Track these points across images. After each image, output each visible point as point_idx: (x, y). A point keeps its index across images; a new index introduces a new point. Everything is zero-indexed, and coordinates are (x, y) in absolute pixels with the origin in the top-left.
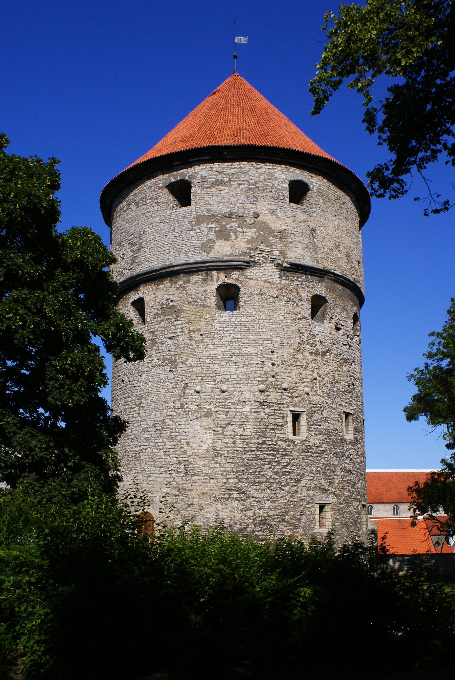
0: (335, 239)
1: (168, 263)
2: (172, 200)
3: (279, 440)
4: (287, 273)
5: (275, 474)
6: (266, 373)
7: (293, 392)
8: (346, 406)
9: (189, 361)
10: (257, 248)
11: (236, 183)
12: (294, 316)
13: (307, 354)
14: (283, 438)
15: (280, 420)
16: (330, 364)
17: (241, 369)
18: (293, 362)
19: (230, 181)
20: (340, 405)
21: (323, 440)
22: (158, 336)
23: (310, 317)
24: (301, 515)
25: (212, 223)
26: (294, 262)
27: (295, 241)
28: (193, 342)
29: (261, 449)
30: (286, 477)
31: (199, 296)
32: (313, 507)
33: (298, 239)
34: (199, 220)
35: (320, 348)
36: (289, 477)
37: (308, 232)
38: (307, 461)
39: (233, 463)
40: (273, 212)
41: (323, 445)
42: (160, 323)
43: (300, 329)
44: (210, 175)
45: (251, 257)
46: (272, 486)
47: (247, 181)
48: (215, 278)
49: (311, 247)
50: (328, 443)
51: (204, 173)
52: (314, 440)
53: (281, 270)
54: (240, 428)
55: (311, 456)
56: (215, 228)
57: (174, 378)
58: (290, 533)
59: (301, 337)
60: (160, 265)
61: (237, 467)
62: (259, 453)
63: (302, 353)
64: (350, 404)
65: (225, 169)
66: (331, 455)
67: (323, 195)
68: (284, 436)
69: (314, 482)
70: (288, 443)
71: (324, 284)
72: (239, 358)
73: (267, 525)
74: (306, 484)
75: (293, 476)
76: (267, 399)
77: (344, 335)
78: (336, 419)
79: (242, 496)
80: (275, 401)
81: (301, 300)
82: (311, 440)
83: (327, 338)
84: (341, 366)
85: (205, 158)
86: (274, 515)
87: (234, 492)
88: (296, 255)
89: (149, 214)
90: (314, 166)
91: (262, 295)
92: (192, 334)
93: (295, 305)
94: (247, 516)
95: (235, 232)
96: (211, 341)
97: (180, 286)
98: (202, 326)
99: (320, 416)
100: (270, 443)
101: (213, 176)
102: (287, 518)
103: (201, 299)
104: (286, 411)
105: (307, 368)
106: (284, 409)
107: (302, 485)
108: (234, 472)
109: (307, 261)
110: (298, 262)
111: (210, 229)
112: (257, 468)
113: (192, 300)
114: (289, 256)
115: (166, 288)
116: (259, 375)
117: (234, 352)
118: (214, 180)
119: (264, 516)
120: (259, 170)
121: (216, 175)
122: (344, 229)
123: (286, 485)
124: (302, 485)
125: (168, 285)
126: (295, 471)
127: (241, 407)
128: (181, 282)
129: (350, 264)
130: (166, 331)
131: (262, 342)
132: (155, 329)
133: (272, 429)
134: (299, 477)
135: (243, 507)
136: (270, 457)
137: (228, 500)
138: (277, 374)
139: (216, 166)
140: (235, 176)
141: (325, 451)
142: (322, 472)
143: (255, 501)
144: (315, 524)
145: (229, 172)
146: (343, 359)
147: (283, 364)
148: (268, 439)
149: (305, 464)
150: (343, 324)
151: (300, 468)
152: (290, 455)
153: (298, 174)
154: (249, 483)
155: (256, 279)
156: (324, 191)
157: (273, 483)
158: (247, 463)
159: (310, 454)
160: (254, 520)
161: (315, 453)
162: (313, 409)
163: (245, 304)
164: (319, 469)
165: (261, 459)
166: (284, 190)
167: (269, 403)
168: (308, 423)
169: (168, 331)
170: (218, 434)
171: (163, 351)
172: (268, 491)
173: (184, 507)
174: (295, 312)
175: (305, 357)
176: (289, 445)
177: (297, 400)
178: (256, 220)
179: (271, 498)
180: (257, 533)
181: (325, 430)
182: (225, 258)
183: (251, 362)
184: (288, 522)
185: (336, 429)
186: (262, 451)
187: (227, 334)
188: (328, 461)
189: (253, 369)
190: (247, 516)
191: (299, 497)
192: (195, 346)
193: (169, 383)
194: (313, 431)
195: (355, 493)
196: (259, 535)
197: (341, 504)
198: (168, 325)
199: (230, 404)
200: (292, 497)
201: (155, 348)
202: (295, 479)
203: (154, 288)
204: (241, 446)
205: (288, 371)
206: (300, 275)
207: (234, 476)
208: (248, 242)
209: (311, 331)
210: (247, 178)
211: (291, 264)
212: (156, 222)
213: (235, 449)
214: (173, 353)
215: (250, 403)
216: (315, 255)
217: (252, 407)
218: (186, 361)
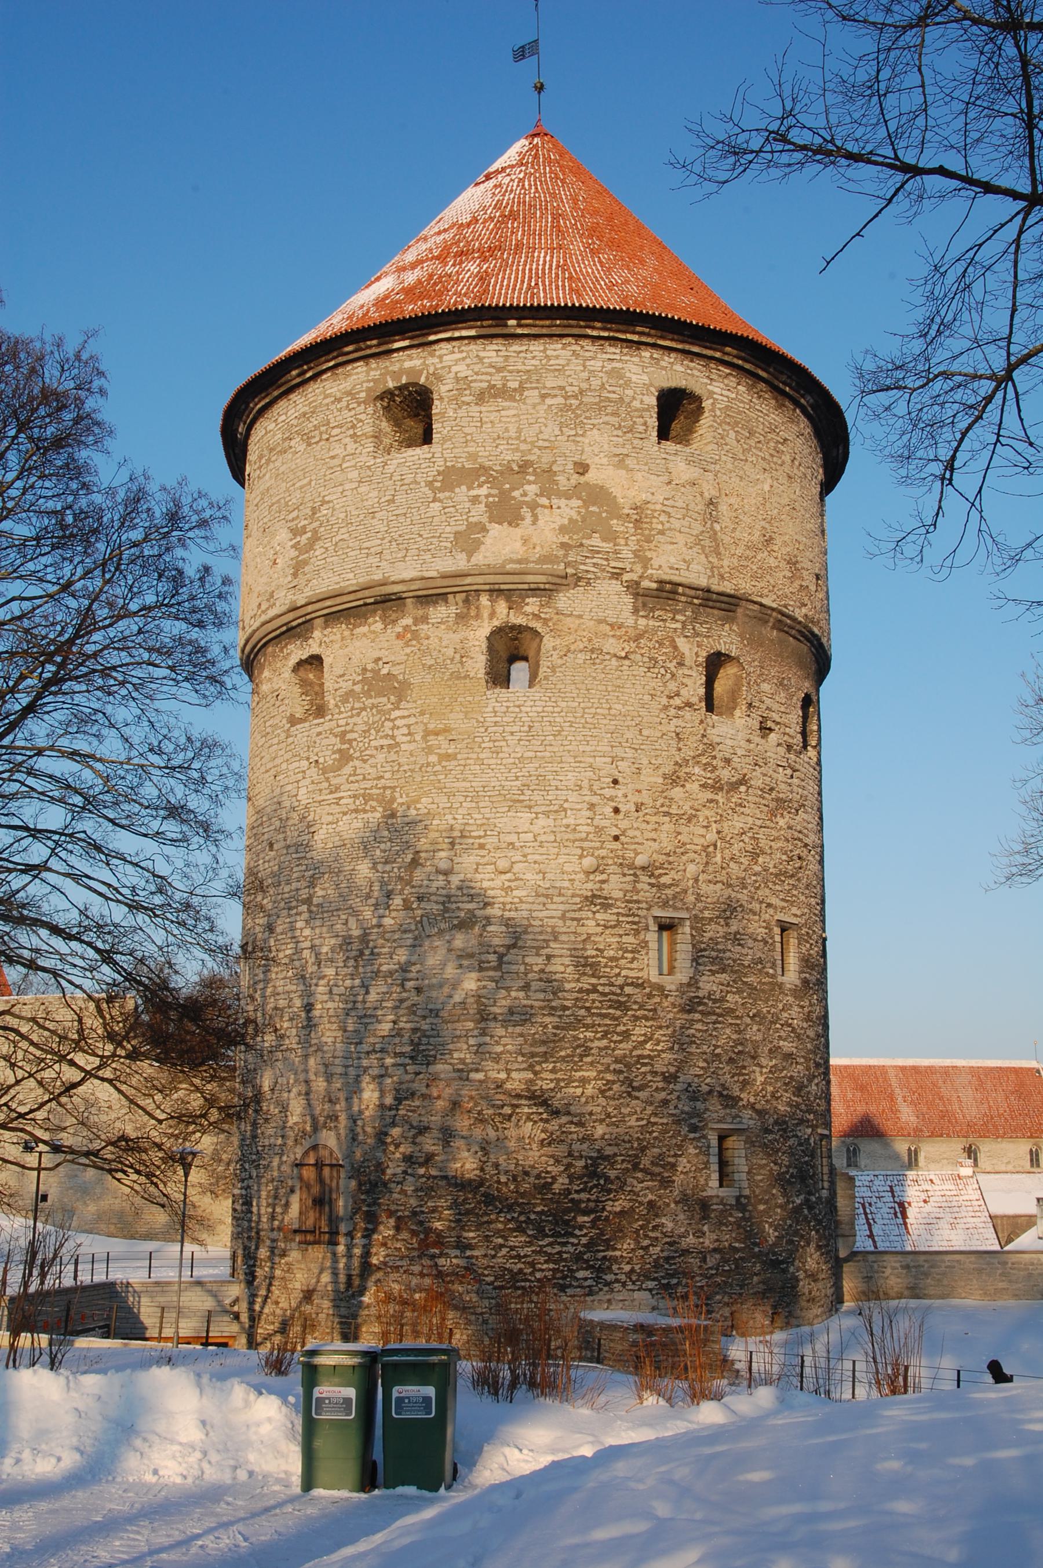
0: (763, 523)
1: (378, 576)
2: (389, 430)
3: (628, 985)
5: (617, 1061)
6: (599, 830)
7: (660, 875)
8: (783, 908)
9: (423, 800)
10: (582, 545)
11: (536, 393)
12: (664, 701)
13: (695, 786)
14: (638, 978)
15: (630, 939)
16: (746, 811)
17: (542, 821)
18: (662, 806)
19: (521, 389)
20: (769, 905)
22: (354, 744)
23: (703, 704)
24: (676, 1155)
25: (480, 486)
26: (667, 578)
27: (670, 529)
28: (433, 758)
29: (587, 1005)
30: (643, 1069)
31: (450, 652)
33: (676, 524)
34: (451, 478)
35: (725, 774)
36: (648, 1068)
37: (700, 507)
38: (692, 1031)
39: (521, 1035)
40: (621, 461)
41: (729, 997)
42: (358, 715)
43: (678, 730)
44: (477, 374)
45: (567, 565)
46: (610, 1089)
47: (562, 388)
48: (486, 614)
49: (707, 543)
50: (739, 992)
51: (462, 370)
53: (636, 595)
54: (538, 955)
55: (700, 1021)
56: (487, 496)
57: (390, 840)
58: (650, 1197)
59: (680, 750)
60: (361, 580)
61: (531, 1045)
62: (582, 1012)
63: (683, 786)
65: (511, 360)
67: (737, 423)
68: (640, 974)
69: (708, 1080)
70: (648, 990)
71: (735, 628)
72: (537, 797)
73: (599, 1178)
74: (689, 1085)
76: (601, 889)
77: (779, 745)
79: (541, 1110)
80: (621, 894)
81: (681, 664)
82: (701, 984)
83: (740, 752)
84: (773, 814)
85: (465, 333)
86: (615, 1155)
87: (523, 1102)
88: (673, 560)
89: (337, 462)
90: (718, 355)
91: (592, 651)
92: (433, 741)
93: (669, 676)
94: (552, 1156)
95: (533, 506)
96: (475, 756)
97: (406, 628)
98: (455, 720)
100: (607, 990)
101: (484, 377)
102: (645, 1162)
103: (452, 660)
104: (645, 917)
105: (694, 820)
106: (640, 912)
108: (523, 1055)
109: (698, 575)
110: (676, 579)
111: (475, 500)
112: (578, 1046)
113: (432, 662)
114: (655, 563)
115: (374, 632)
116: (584, 835)
117: (525, 780)
118: (485, 385)
119: (591, 1158)
120: (588, 363)
121: (490, 374)
122: (786, 501)
123: (639, 1089)
124: (678, 1087)
125: (379, 626)
126: (663, 1055)
127: (541, 907)
128: (408, 621)
129: (797, 584)
130: (373, 731)
131: (591, 760)
132: (348, 728)
133: (612, 959)
134: (672, 1070)
135: (543, 1136)
137: (509, 1120)
138: (623, 834)
139: (492, 352)
140: (534, 377)
141: (733, 1011)
142: (725, 1058)
143: (572, 1123)
144: (709, 1176)
145: (522, 368)
148: (602, 981)
149: (687, 1040)
150: (778, 720)
151: (676, 1047)
152: (653, 1019)
153: (678, 371)
154: (558, 1080)
155: (580, 617)
156: (740, 413)
157: (614, 1082)
158: (555, 1035)
159: (697, 1016)
160: (569, 1166)
161: (709, 1014)
163: (554, 671)
165: (587, 1027)
166: (647, 410)
167: (606, 898)
168: (694, 946)
169: (378, 732)
170: (487, 969)
171: (364, 779)
172: (602, 1101)
173: (411, 1134)
174: (666, 693)
175: (690, 794)
176: (650, 996)
177: (668, 891)
178: (582, 479)
179: (608, 1116)
180: (576, 1196)
181: (734, 961)
182: (509, 567)
183: (566, 805)
184: (644, 1171)
185: (760, 961)
186: (588, 1009)
187: (512, 740)
188: (739, 1032)
189: (571, 821)
190: (552, 1156)
191: (672, 1115)
192: (438, 768)
193: (378, 852)
195: (803, 1107)
196: (580, 1201)
197: (767, 1131)
198: (376, 718)
199: (516, 900)
200: (656, 1115)
201: (347, 770)
202: (663, 1073)
203: (347, 633)
204: (541, 996)
205: (650, 827)
206: (680, 606)
207: (524, 1065)
208: (563, 530)
209: (704, 736)
210: (561, 382)
211: (660, 582)
212: (351, 481)
213: (525, 1002)
214: (389, 784)
215: (562, 899)
216: (714, 560)
217: (567, 907)
218: (418, 801)
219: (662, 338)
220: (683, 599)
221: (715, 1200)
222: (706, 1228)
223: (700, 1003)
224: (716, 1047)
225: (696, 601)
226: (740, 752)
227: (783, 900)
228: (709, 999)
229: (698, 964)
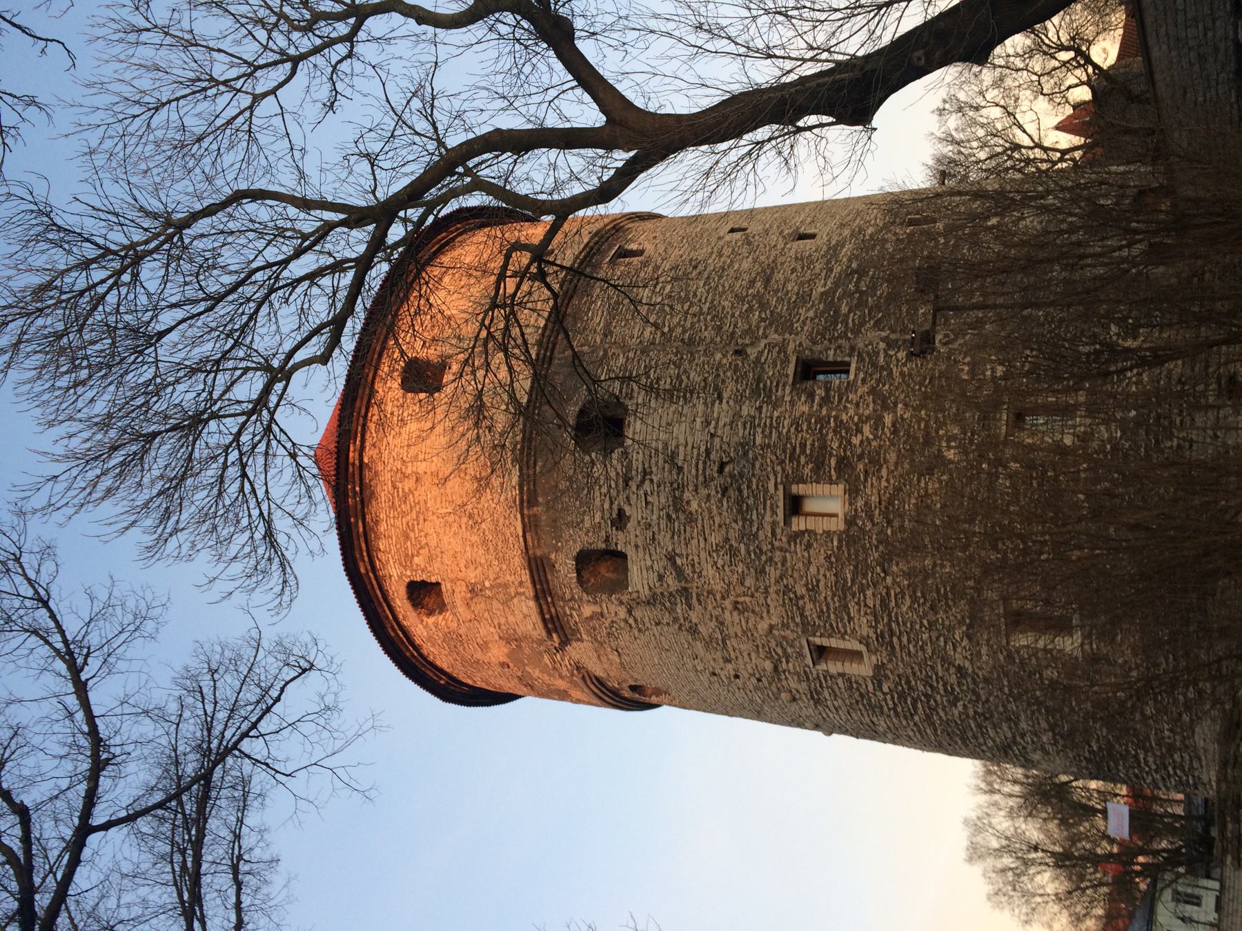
4: (568, 632)
20: (774, 533)
21: (858, 604)
32: (1018, 651)
41: (870, 603)
45: (572, 675)
50: (862, 590)
52: (865, 631)
64: (766, 491)
66: (889, 580)
75: (953, 679)
78: (806, 554)
82: (865, 634)
83: (649, 563)
84: (691, 519)
99: (809, 606)
107: (967, 664)
124: (967, 664)
134: (952, 670)
136: (919, 705)
142: (931, 617)
146: (677, 511)
147: (727, 660)
149: (920, 653)
159: (895, 640)
161: (891, 630)
162: (798, 620)
164: (925, 622)
181: (834, 595)
185: (828, 557)
194: (844, 626)
219: (387, 617)
220: (553, 610)
221: (1087, 647)
222: (1120, 661)
223: (883, 637)
224: (922, 625)
226: (649, 563)
227: (765, 509)
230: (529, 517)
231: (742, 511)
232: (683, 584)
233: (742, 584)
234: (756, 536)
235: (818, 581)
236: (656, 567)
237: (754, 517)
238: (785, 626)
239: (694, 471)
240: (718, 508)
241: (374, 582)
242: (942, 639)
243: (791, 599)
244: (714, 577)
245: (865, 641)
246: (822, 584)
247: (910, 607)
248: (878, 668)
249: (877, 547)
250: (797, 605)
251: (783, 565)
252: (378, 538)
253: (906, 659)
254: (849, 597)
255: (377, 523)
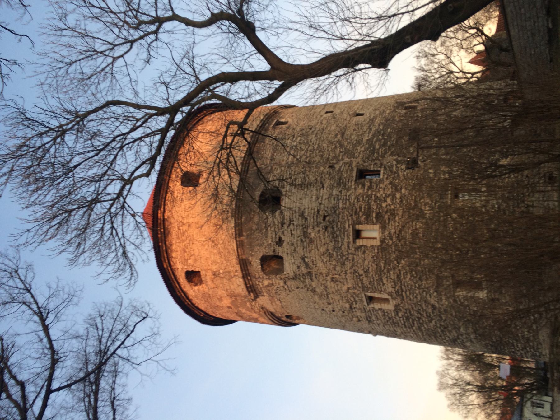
4: (258, 292)
10: (252, 308)
20: (348, 247)
21: (387, 277)
41: (392, 277)
45: (260, 311)
50: (389, 271)
52: (390, 290)
64: (345, 228)
75: (430, 310)
78: (363, 256)
83: (293, 261)
84: (311, 241)
99: (365, 279)
134: (430, 307)
136: (415, 322)
141: (398, 276)
142: (420, 283)
146: (305, 237)
147: (329, 304)
149: (415, 299)
159: (404, 293)
161: (402, 289)
162: (360, 285)
164: (417, 285)
181: (376, 274)
185: (373, 257)
194: (381, 288)
219: (177, 287)
220: (251, 282)
224: (416, 287)
225: (249, 278)
227: (344, 236)
228: (395, 288)
229: (381, 291)
230: (239, 241)
231: (334, 237)
232: (309, 270)
233: (335, 269)
234: (340, 248)
235: (369, 268)
236: (296, 262)
237: (340, 240)
238: (355, 288)
239: (312, 220)
240: (324, 236)
241: (170, 272)
242: (425, 293)
243: (357, 276)
244: (322, 267)
245: (390, 294)
246: (370, 269)
247: (410, 279)
248: (397, 306)
249: (394, 252)
250: (359, 278)
251: (353, 261)
252: (172, 252)
253: (409, 301)
254: (383, 275)
255: (171, 245)
